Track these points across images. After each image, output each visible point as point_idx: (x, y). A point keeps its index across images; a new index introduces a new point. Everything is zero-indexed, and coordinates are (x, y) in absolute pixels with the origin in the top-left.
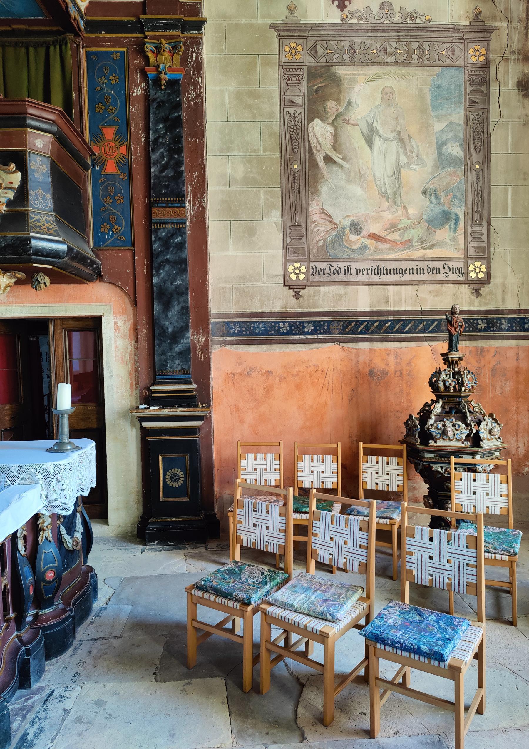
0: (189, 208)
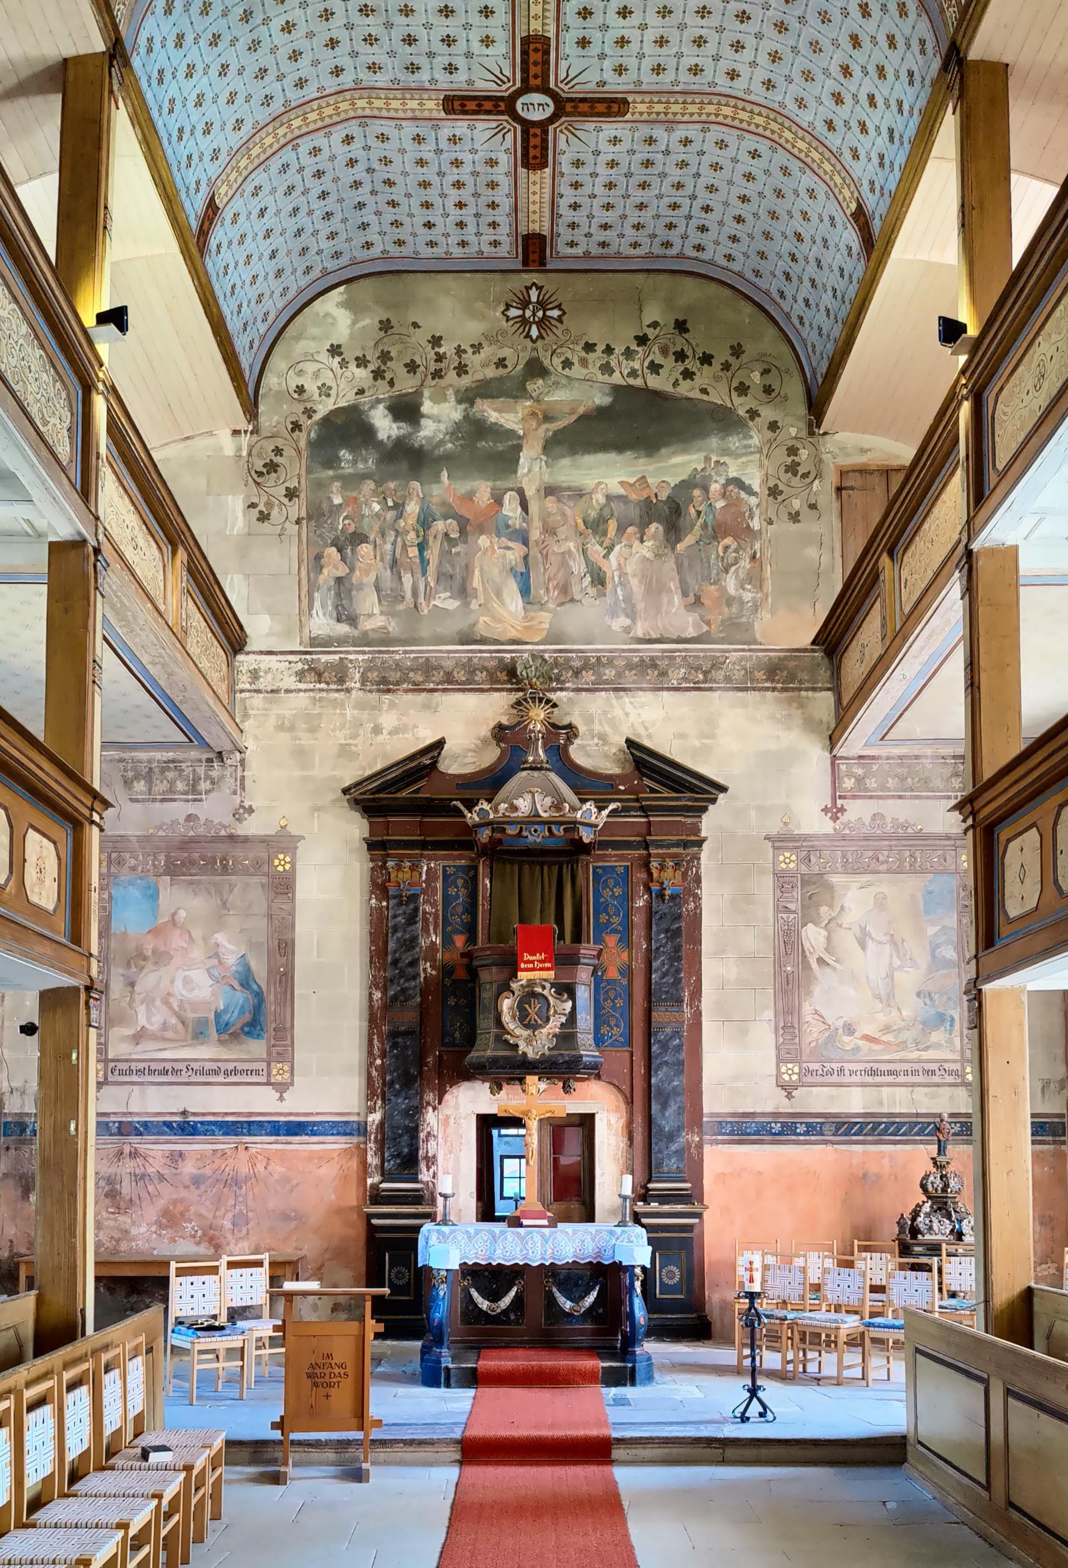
0: (686, 1009)
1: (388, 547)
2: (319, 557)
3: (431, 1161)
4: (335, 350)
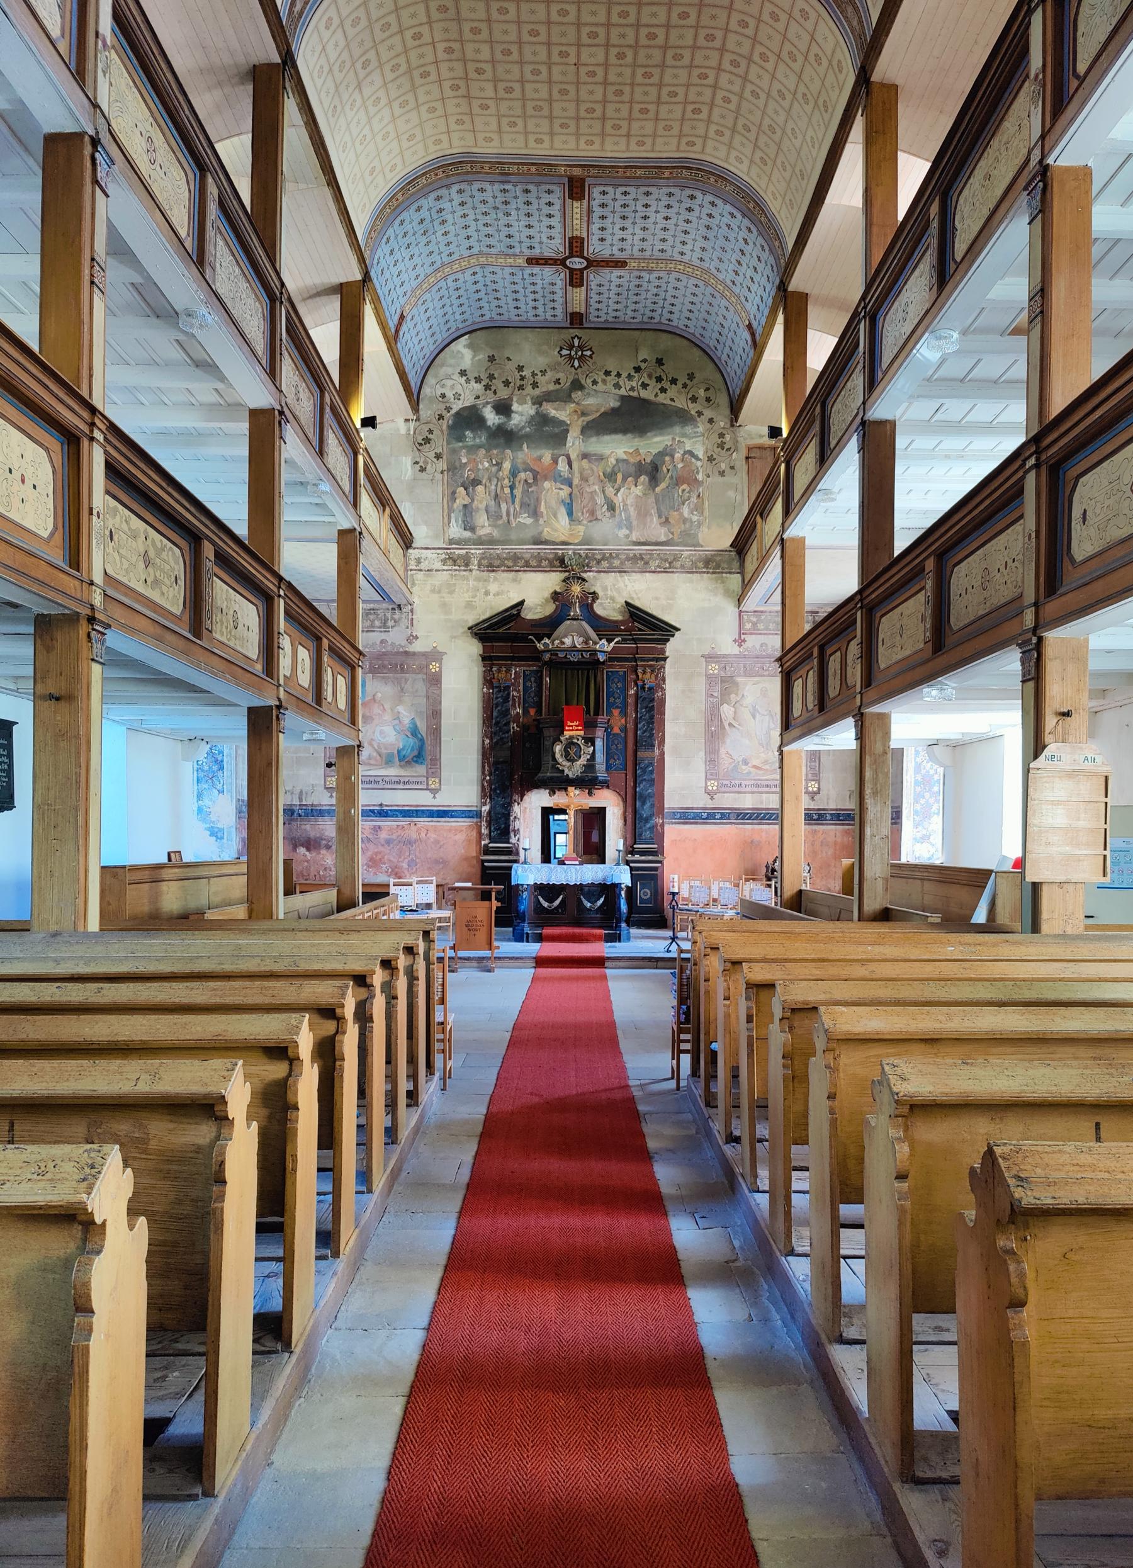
0: (656, 751)
1: (493, 487)
2: (454, 493)
3: (516, 832)
4: (463, 373)
